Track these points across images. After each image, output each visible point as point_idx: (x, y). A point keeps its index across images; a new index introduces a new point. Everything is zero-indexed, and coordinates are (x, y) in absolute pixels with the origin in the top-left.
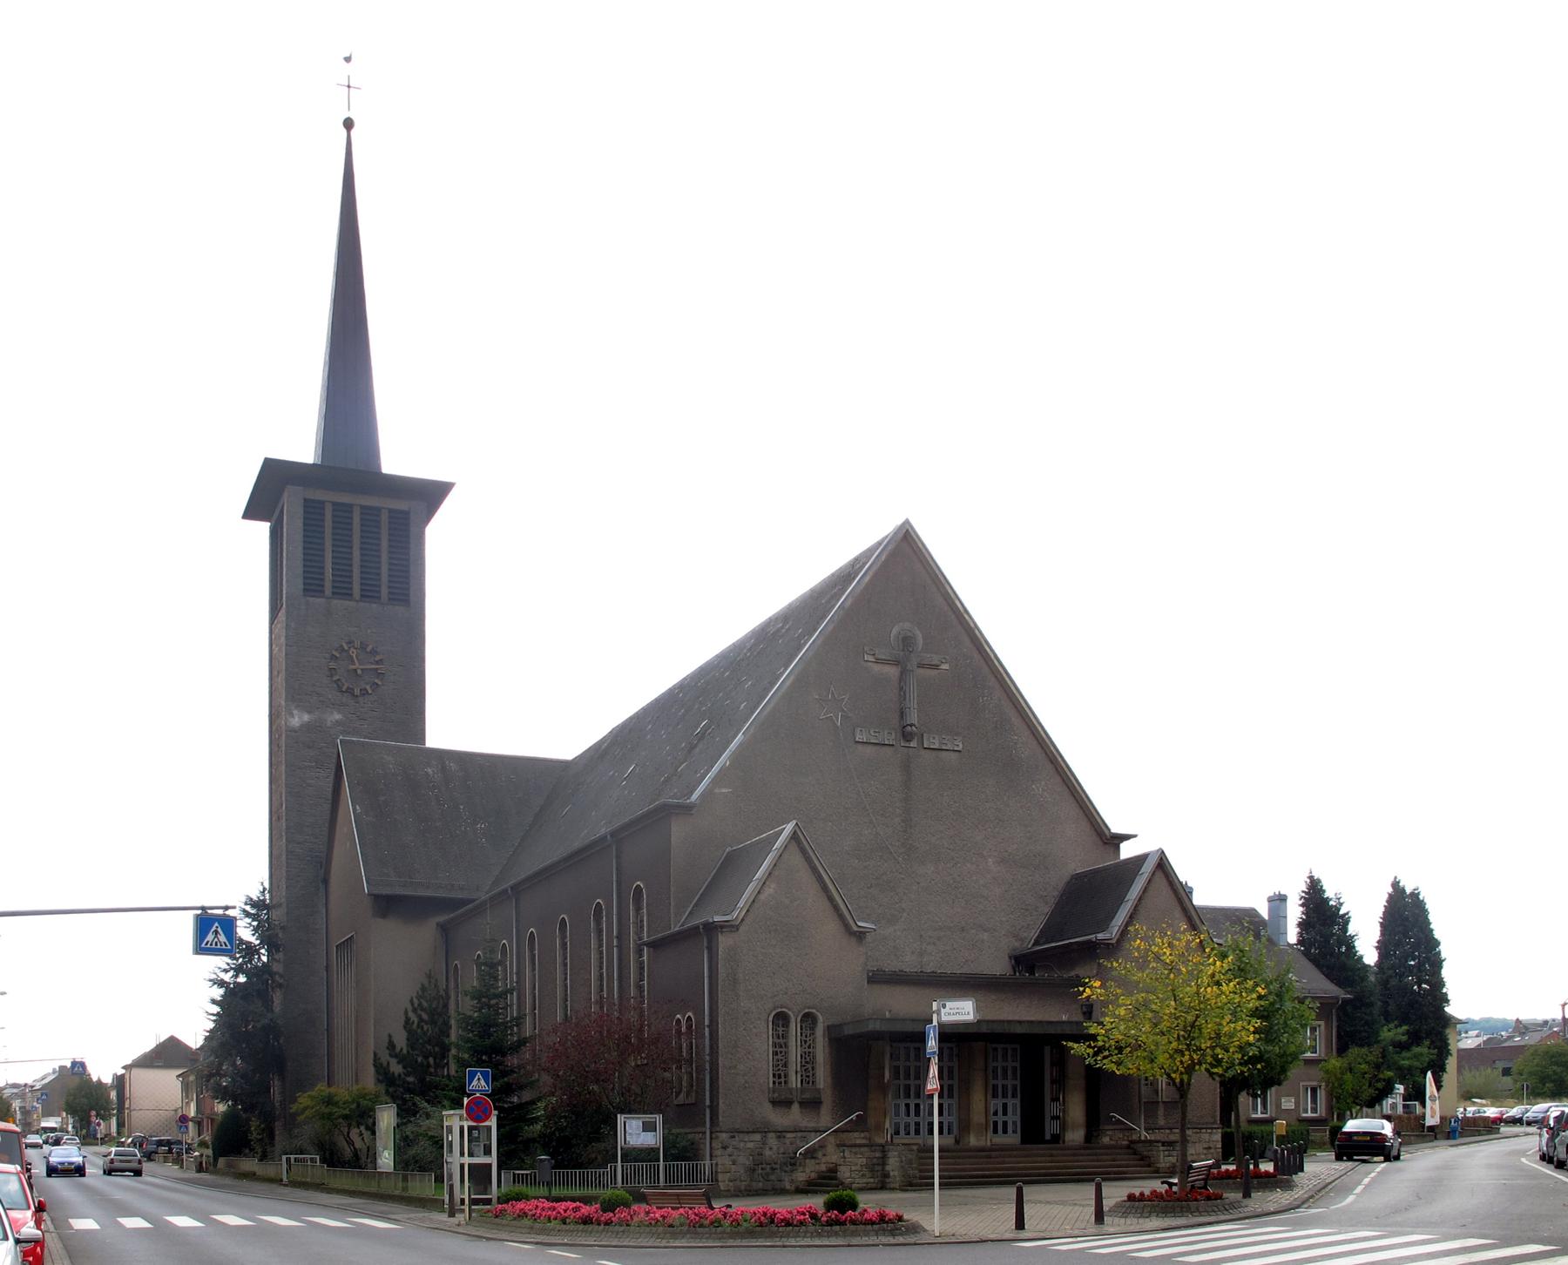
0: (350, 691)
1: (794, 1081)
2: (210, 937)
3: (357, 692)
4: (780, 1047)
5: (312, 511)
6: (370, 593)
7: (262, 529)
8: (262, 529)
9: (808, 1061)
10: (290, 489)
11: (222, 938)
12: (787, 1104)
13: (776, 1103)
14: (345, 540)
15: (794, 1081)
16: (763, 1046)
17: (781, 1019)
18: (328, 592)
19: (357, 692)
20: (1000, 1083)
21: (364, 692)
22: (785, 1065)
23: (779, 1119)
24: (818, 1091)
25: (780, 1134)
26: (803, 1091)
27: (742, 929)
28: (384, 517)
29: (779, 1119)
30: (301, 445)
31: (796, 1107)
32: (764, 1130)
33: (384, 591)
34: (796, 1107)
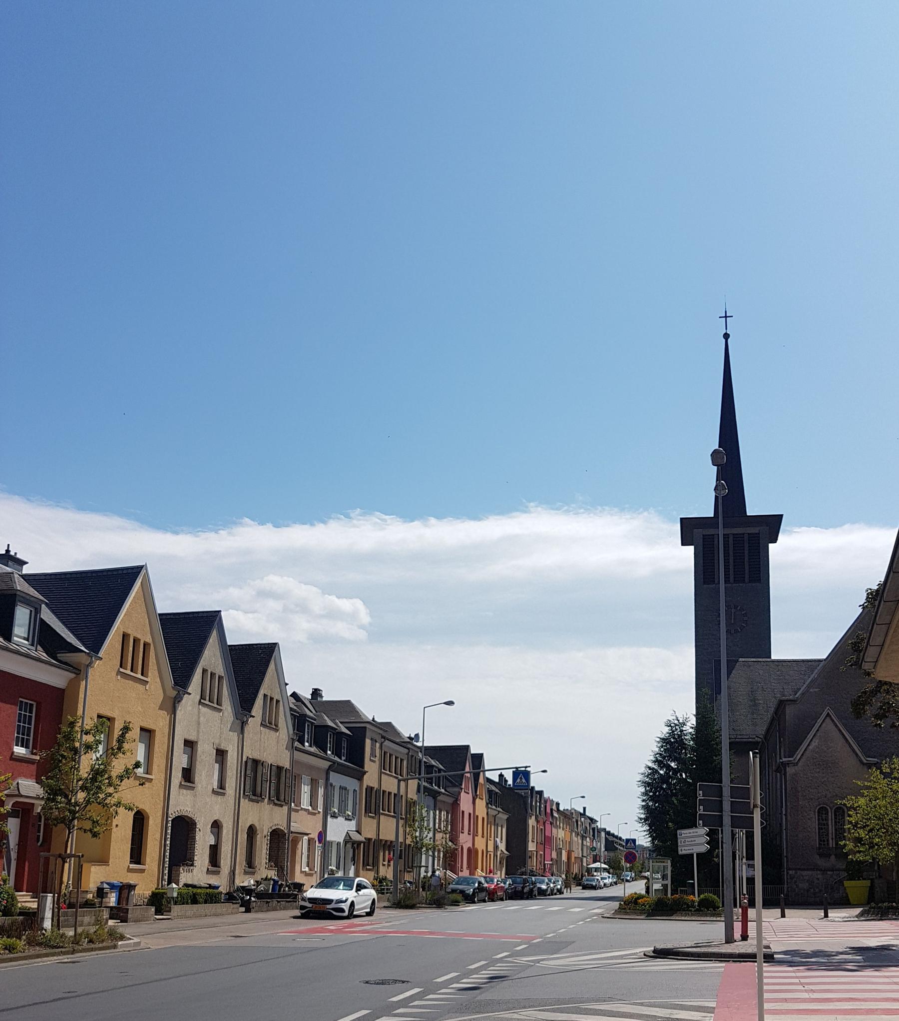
2: (518, 780)
3: (733, 632)
4: (823, 826)
7: (690, 549)
8: (690, 549)
11: (524, 781)
13: (821, 855)
14: (731, 552)
16: (813, 824)
17: (822, 811)
19: (733, 632)
21: (736, 631)
22: (827, 835)
23: (821, 862)
25: (824, 871)
27: (800, 764)
29: (821, 862)
30: (704, 507)
31: (833, 857)
32: (815, 868)
33: (747, 576)
34: (833, 857)
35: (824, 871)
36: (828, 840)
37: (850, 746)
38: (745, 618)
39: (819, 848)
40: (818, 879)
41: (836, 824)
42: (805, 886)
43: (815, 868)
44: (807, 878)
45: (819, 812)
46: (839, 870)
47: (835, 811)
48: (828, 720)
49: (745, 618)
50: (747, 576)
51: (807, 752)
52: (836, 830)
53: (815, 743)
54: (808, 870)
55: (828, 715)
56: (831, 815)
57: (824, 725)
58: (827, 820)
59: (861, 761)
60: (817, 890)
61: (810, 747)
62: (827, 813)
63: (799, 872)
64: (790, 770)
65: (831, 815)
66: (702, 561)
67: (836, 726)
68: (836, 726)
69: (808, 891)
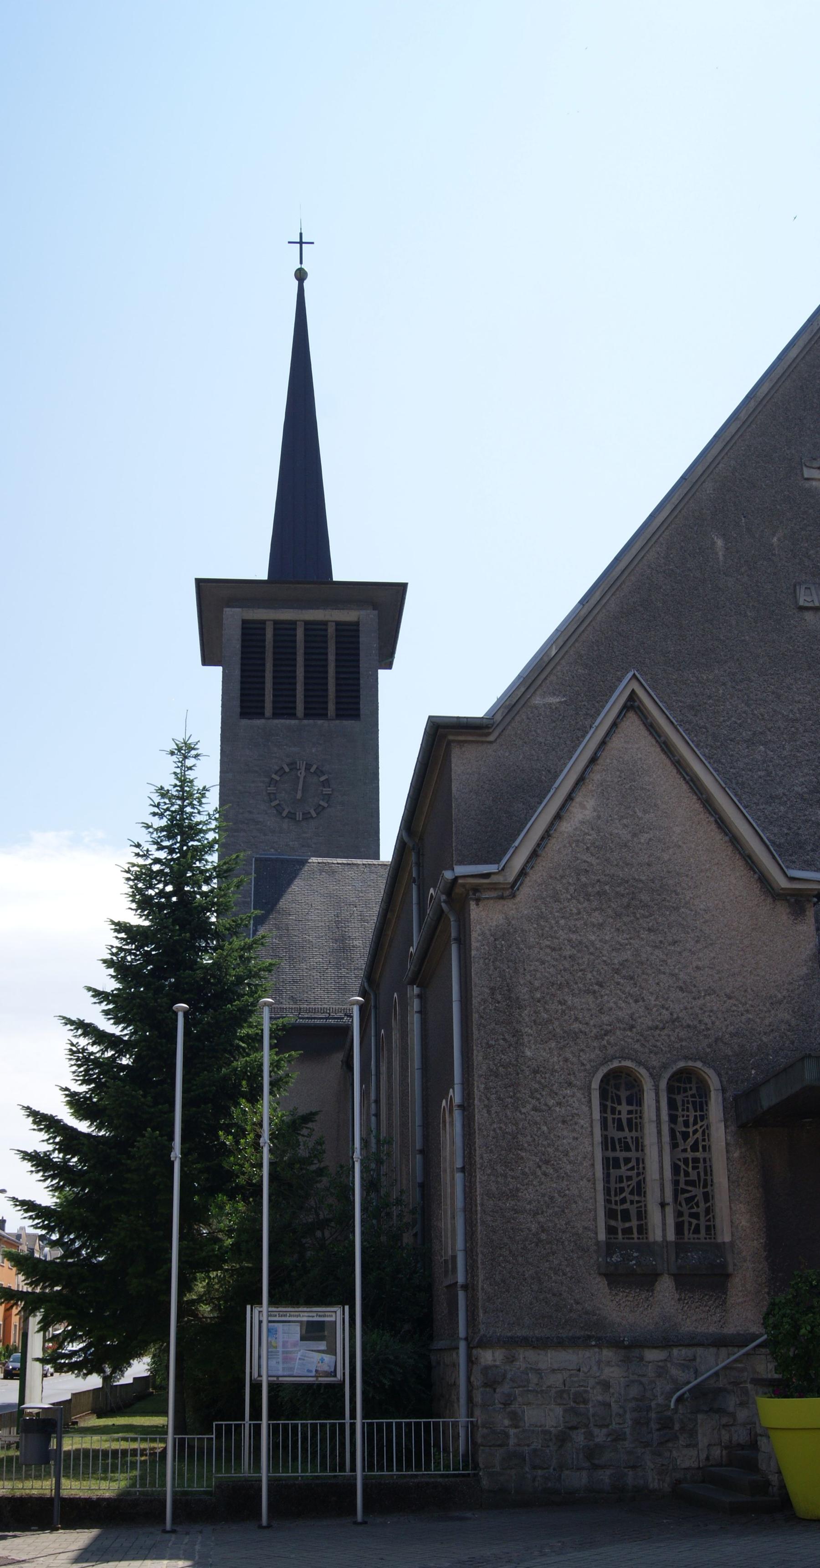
0: (291, 816)
1: (660, 1226)
3: (299, 816)
5: (251, 632)
6: (315, 710)
9: (691, 1183)
10: (228, 611)
12: (646, 1280)
13: (617, 1278)
15: (660, 1226)
16: (581, 1138)
17: (619, 1087)
19: (299, 816)
21: (307, 816)
22: (640, 1189)
23: (619, 1310)
24: (719, 1247)
25: (629, 1346)
26: (680, 1247)
27: (526, 891)
28: (331, 630)
29: (619, 1310)
31: (666, 1286)
32: (593, 1335)
33: (331, 707)
34: (666, 1286)
35: (629, 1346)
36: (642, 1215)
37: (722, 824)
38: (327, 791)
39: (610, 1248)
40: (606, 1385)
41: (674, 1146)
42: (544, 1416)
43: (593, 1335)
44: (555, 1380)
45: (604, 1094)
46: (693, 1342)
47: (670, 1090)
48: (632, 723)
49: (327, 791)
50: (331, 707)
51: (554, 845)
52: (676, 1169)
53: (584, 810)
54: (561, 1344)
55: (632, 704)
56: (653, 1105)
57: (616, 742)
58: (635, 1124)
59: (764, 881)
60: (600, 1436)
61: (566, 827)
62: (636, 1099)
63: (526, 1357)
64: (484, 918)
65: (653, 1105)
66: (237, 673)
67: (667, 748)
68: (667, 748)
69: (562, 1438)
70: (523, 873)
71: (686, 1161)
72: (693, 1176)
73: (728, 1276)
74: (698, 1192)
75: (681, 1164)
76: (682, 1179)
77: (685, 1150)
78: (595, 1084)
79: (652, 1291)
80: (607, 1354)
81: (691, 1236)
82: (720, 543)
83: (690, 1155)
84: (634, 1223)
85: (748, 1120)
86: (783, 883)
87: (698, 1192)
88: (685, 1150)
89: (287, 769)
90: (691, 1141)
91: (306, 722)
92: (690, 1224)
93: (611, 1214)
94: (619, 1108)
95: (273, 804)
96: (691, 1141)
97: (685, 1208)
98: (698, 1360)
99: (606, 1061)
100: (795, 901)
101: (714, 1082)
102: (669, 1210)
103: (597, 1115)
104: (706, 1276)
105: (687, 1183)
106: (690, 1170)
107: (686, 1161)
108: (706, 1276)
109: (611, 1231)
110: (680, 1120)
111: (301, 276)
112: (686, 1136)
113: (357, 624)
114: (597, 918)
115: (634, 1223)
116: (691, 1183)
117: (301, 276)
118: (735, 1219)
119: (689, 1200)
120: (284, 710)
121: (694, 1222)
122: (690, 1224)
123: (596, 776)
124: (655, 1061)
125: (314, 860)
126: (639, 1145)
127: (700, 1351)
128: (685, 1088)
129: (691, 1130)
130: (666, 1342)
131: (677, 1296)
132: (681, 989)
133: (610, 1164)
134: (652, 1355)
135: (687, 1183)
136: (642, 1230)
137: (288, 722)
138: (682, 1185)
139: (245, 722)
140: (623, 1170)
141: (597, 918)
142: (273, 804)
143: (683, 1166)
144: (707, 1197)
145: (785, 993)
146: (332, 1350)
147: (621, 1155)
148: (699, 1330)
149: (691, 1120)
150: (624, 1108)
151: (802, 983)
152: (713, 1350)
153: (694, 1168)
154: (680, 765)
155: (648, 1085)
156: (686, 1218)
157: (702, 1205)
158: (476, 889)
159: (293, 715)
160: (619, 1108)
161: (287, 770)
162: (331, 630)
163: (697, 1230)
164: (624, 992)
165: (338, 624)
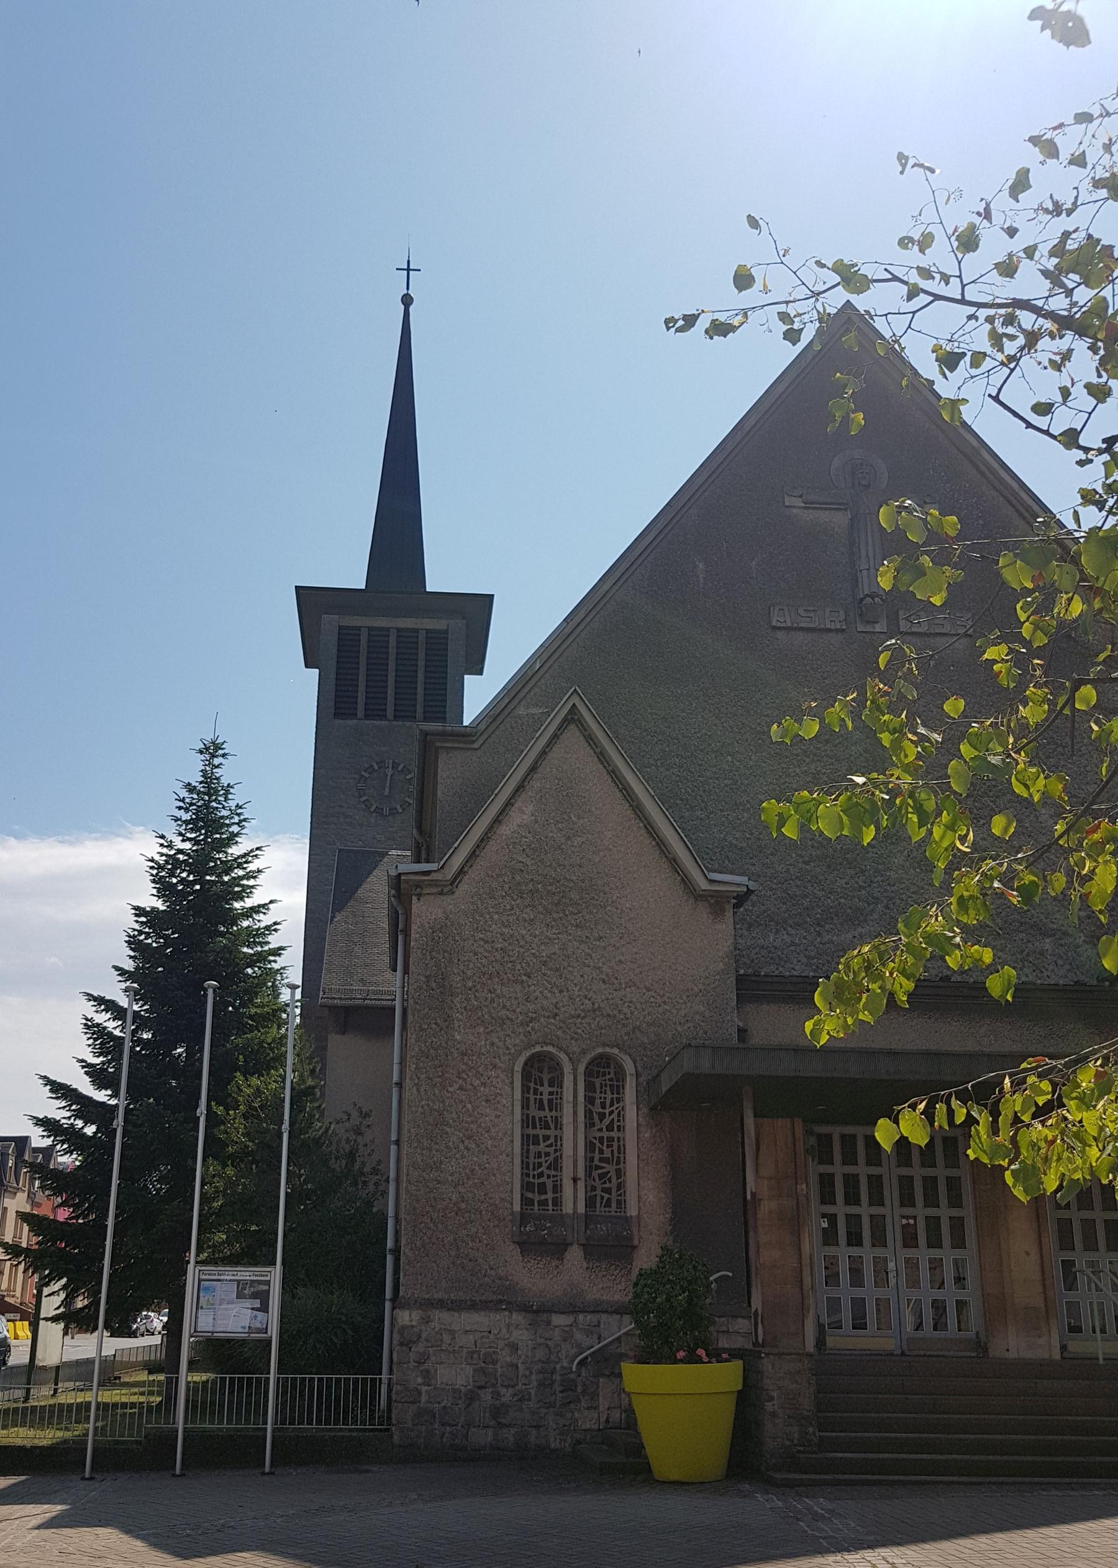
1: (573, 1200)
3: (386, 811)
4: (539, 1126)
5: (347, 638)
9: (604, 1159)
12: (558, 1249)
13: (528, 1246)
15: (573, 1200)
17: (540, 1070)
18: (361, 712)
19: (386, 811)
20: (838, 1170)
21: (393, 812)
22: (556, 1165)
23: (531, 1277)
24: (627, 1220)
25: (537, 1311)
26: (588, 1219)
27: (464, 888)
28: (422, 636)
29: (531, 1277)
31: (575, 1254)
32: (504, 1299)
33: (420, 709)
34: (575, 1254)
35: (537, 1311)
36: (557, 1188)
37: (651, 830)
39: (524, 1218)
40: (514, 1347)
41: (590, 1124)
42: (455, 1375)
43: (504, 1299)
44: (467, 1341)
45: (526, 1076)
46: (598, 1309)
47: (588, 1073)
48: (572, 734)
50: (420, 709)
51: (492, 846)
52: (590, 1147)
53: (523, 815)
54: (473, 1307)
55: (573, 718)
56: (572, 1089)
57: (557, 752)
58: (555, 1105)
59: (686, 882)
60: (507, 1395)
61: (505, 830)
62: (557, 1082)
63: (441, 1317)
65: (572, 1089)
66: (333, 676)
67: (602, 757)
68: (602, 757)
69: (471, 1397)
70: (461, 872)
71: (601, 1140)
72: (607, 1154)
73: (634, 1247)
74: (611, 1168)
75: (596, 1142)
76: (597, 1156)
77: (601, 1130)
78: (518, 1067)
79: (562, 1259)
80: (517, 1317)
81: (603, 1209)
82: (701, 566)
83: (605, 1134)
84: (550, 1196)
85: (661, 1106)
86: (704, 885)
87: (611, 1168)
88: (601, 1130)
89: (376, 767)
90: (607, 1121)
91: (395, 723)
92: (602, 1198)
93: (527, 1186)
94: (541, 1089)
95: (362, 799)
96: (607, 1121)
97: (598, 1183)
98: (602, 1326)
99: (530, 1045)
100: (716, 902)
101: (629, 1067)
102: (581, 1184)
103: (518, 1095)
104: (611, 1246)
105: (601, 1160)
106: (605, 1148)
107: (601, 1140)
108: (611, 1246)
109: (526, 1202)
110: (598, 1101)
111: (407, 300)
112: (602, 1117)
113: (446, 632)
114: (529, 914)
115: (550, 1196)
116: (604, 1159)
117: (407, 300)
118: (645, 1196)
119: (601, 1176)
120: (375, 711)
121: (606, 1196)
122: (602, 1198)
123: (536, 784)
124: (575, 1048)
125: (394, 852)
126: (558, 1125)
127: (604, 1317)
128: (602, 1072)
129: (607, 1111)
130: (572, 1309)
131: (585, 1265)
132: (604, 982)
133: (528, 1141)
134: (558, 1320)
135: (601, 1160)
136: (557, 1202)
137: (378, 723)
138: (596, 1162)
139: (338, 722)
140: (542, 1147)
141: (529, 914)
142: (362, 799)
143: (598, 1144)
144: (619, 1173)
145: (701, 986)
146: (264, 1308)
147: (541, 1133)
148: (604, 1298)
149: (608, 1102)
150: (546, 1089)
151: (718, 977)
152: (616, 1317)
153: (608, 1146)
154: (614, 775)
155: (567, 1068)
156: (599, 1192)
157: (614, 1180)
158: (418, 885)
159: (384, 717)
160: (541, 1089)
161: (376, 767)
162: (422, 636)
163: (608, 1204)
164: (550, 983)
165: (428, 631)
